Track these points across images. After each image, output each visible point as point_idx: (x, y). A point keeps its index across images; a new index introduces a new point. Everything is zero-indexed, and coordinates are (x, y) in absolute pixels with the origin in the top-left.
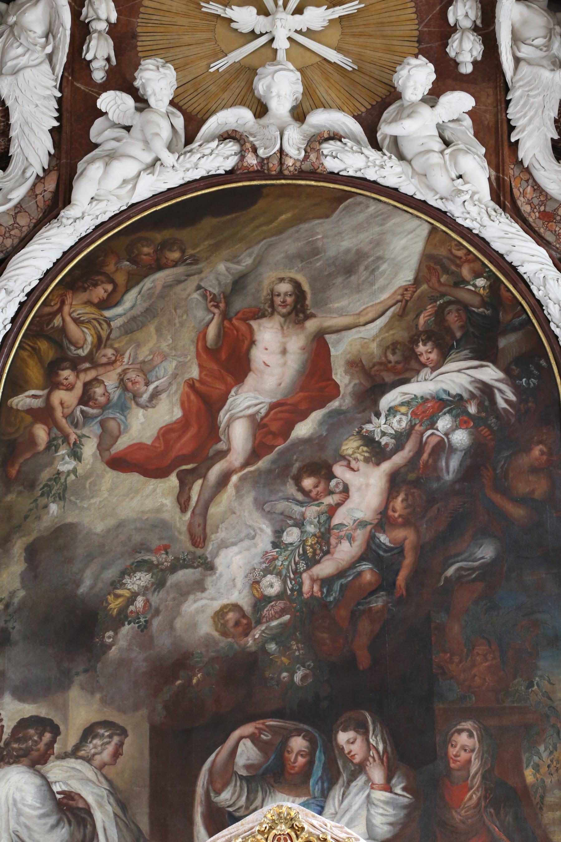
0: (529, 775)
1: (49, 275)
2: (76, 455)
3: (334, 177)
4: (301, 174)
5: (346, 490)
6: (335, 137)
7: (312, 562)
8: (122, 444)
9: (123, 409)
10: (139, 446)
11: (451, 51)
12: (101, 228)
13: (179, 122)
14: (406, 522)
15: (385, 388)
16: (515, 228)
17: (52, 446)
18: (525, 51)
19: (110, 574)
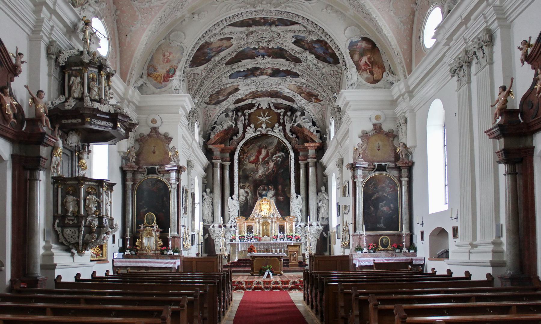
0: (285, 190)
1: (243, 145)
2: (246, 162)
3: (269, 134)
4: (266, 134)
6: (269, 131)
7: (267, 171)
8: (250, 161)
10: (251, 161)
11: (280, 121)
12: (248, 140)
13: (255, 129)
14: (275, 168)
15: (274, 155)
17: (244, 161)
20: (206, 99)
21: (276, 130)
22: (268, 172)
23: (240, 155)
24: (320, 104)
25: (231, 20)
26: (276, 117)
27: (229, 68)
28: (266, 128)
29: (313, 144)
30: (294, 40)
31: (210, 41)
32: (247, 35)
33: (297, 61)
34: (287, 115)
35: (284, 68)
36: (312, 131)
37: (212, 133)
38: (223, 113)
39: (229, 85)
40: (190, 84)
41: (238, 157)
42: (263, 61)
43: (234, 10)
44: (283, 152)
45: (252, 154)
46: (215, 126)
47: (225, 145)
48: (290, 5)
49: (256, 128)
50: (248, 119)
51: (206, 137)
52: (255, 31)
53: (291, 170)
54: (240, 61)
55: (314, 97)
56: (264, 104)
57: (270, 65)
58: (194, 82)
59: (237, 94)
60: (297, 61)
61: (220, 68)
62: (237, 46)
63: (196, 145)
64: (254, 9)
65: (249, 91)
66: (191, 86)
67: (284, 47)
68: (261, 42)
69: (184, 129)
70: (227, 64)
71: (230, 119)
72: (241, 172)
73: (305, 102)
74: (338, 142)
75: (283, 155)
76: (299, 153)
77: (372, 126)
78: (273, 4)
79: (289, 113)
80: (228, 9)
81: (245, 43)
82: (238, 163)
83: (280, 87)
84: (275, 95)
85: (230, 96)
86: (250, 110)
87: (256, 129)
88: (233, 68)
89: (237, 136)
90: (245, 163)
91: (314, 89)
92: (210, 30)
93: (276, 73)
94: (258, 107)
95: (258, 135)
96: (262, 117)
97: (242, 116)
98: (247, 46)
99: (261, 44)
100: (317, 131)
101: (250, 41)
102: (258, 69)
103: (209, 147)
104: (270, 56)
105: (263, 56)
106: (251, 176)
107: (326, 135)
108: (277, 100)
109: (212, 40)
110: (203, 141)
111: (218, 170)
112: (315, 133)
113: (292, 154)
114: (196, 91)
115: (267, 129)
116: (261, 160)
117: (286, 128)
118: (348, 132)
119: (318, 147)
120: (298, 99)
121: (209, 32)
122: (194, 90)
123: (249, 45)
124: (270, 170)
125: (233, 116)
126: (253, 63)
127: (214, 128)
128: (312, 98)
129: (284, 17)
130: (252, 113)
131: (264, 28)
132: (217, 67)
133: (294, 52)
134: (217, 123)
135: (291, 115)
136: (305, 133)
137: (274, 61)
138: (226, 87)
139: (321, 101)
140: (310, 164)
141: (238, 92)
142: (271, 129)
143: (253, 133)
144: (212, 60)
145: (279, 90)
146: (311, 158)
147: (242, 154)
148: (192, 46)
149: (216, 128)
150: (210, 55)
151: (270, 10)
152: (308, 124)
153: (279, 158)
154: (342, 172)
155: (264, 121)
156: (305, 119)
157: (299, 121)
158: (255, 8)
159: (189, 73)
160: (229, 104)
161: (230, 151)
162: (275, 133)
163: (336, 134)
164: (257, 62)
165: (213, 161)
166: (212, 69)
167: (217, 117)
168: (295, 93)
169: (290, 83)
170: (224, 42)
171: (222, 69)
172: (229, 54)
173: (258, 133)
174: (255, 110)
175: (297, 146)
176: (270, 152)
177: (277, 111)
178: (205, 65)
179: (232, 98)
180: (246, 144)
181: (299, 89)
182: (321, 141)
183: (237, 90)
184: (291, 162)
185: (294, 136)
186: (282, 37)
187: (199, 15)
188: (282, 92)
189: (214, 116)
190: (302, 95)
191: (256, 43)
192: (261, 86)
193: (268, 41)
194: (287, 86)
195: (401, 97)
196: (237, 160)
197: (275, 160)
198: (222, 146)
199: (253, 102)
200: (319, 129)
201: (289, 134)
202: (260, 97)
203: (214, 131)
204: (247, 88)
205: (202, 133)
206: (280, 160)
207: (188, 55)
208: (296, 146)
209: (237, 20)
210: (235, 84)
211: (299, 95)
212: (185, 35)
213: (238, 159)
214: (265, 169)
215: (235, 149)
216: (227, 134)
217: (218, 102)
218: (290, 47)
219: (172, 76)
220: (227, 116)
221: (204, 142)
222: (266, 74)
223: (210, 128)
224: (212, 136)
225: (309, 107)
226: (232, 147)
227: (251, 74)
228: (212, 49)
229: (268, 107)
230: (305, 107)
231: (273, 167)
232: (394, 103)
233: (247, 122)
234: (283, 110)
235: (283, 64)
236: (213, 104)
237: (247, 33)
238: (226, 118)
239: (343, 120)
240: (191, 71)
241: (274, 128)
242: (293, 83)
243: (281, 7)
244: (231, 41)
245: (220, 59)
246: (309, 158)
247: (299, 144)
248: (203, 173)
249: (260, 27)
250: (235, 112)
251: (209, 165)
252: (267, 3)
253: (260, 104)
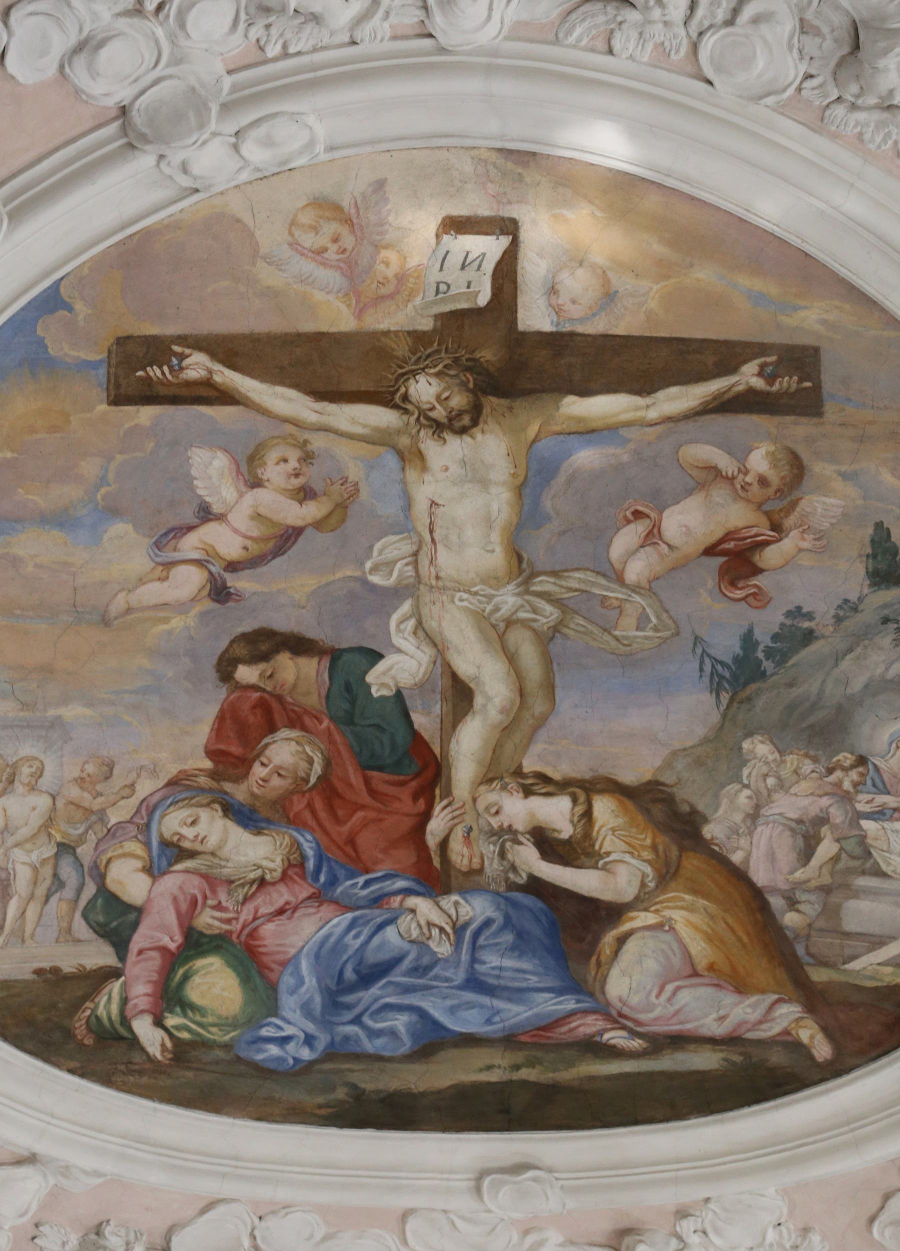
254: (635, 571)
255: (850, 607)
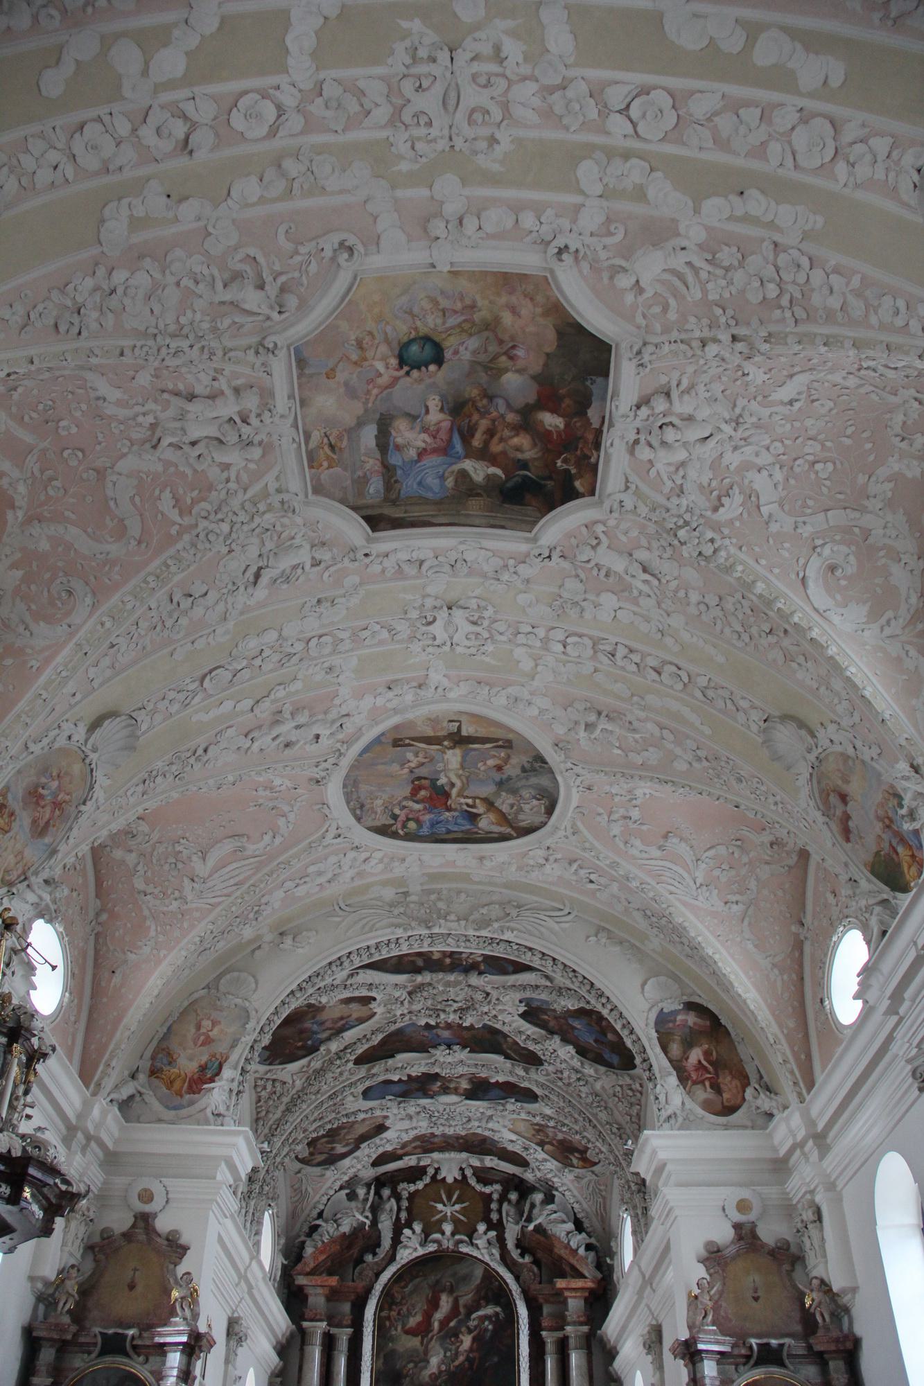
1: (390, 1279)
2: (396, 1330)
3: (461, 1253)
4: (453, 1251)
5: (462, 1342)
6: (462, 1241)
7: (453, 1361)
9: (408, 1317)
12: (403, 1266)
16: (505, 1269)
18: (510, 1219)
19: (404, 1363)
20: (299, 1148)
21: (481, 1242)
22: (457, 1363)
23: (380, 1308)
24: (593, 1172)
25: (371, 954)
26: (481, 1205)
27: (363, 1071)
28: (453, 1234)
29: (579, 1283)
30: (522, 1009)
31: (320, 1002)
32: (410, 993)
33: (532, 1060)
34: (509, 1202)
35: (501, 1079)
36: (573, 1244)
37: (308, 1243)
38: (341, 1188)
39: (361, 1116)
40: (261, 1107)
41: (375, 1314)
42: (449, 1059)
43: (379, 933)
44: (497, 1303)
45: (413, 1306)
46: (317, 1222)
47: (342, 1279)
48: (512, 924)
49: (426, 1233)
50: (407, 1209)
51: (292, 1253)
52: (430, 984)
53: (521, 1359)
54: (392, 1056)
55: (576, 1154)
56: (450, 1171)
57: (466, 1069)
58: (271, 1102)
59: (381, 1139)
60: (532, 1060)
61: (339, 1070)
62: (386, 1018)
63: (259, 1275)
64: (428, 932)
65: (412, 1134)
66: (263, 1113)
67: (498, 1026)
68: (444, 1011)
69: (229, 1223)
70: (359, 1061)
71: (360, 1205)
72: (381, 1361)
73: (553, 1167)
74: (644, 1276)
75: (497, 1314)
76: (540, 1308)
77: (732, 1231)
78: (473, 922)
79: (513, 1196)
80: (367, 928)
81: (406, 1011)
82: (374, 1332)
83: (490, 1125)
84: (478, 1145)
85: (362, 1146)
86: (414, 1183)
87: (427, 1236)
88: (373, 1071)
89: (375, 1254)
90: (394, 1333)
91: (577, 1132)
92: (319, 974)
93: (479, 1089)
94: (434, 1178)
95: (431, 1253)
96: (445, 1205)
97: (393, 1200)
98: (410, 1019)
99: (442, 1016)
100: (589, 1247)
101: (416, 1007)
102: (436, 1076)
103: (296, 1283)
104: (464, 1047)
105: (449, 1047)
106: (407, 1376)
107: (612, 1259)
108: (482, 1161)
109: (324, 1000)
110: (283, 1264)
111: (314, 1351)
112: (582, 1251)
113: (522, 1311)
114: (274, 1127)
115: (457, 1237)
116: (436, 1325)
117: (507, 1235)
118: (667, 1249)
119: (591, 1291)
120: (537, 1160)
121: (315, 980)
122: (270, 1123)
123: (414, 1018)
124: (461, 1358)
125: (367, 1199)
126: (423, 1062)
127: (314, 1228)
128: (571, 1157)
129: (498, 952)
130: (417, 1191)
131: (452, 977)
132: (333, 1068)
133: (524, 1037)
134: (325, 1215)
135: (518, 1202)
136: (556, 1250)
137: (475, 1059)
138: (352, 1119)
139: (595, 1164)
140: (572, 1342)
141: (387, 1135)
142: (466, 1238)
143: (418, 1246)
144: (322, 1049)
145: (487, 1133)
146: (574, 1323)
147: (386, 1306)
148: (272, 1010)
149: (320, 1230)
150: (319, 1036)
151: (466, 936)
152: (564, 1226)
153: (486, 1323)
154: (659, 1366)
155: (449, 1214)
156: (555, 1212)
157: (541, 1218)
158: (429, 928)
159: (262, 1079)
160: (359, 1166)
161: (353, 1297)
162: (478, 1248)
163: (639, 1252)
164: (433, 1060)
165: (305, 1324)
166: (319, 1073)
167: (326, 1198)
168: (528, 1143)
169: (515, 1116)
170: (354, 1006)
171: (346, 1074)
172: (365, 1036)
173: (432, 1248)
174: (426, 1185)
175: (535, 1287)
176: (462, 1302)
177: (483, 1190)
178: (304, 1062)
179: (367, 1151)
180: (398, 1278)
181: (538, 1131)
182: (599, 1276)
183: (381, 1128)
184: (518, 1334)
185: (527, 1259)
186: (494, 1001)
187: (296, 939)
188: (496, 1138)
189: (318, 1196)
190: (547, 1147)
191: (431, 1013)
192: (442, 1121)
193: (461, 1009)
194: (507, 1123)
195: (798, 1152)
196: (371, 1324)
197: (476, 1327)
198: (333, 1281)
199: (422, 1164)
200: (593, 1241)
201: (515, 1254)
202: (441, 1149)
203: (315, 1236)
204: (406, 1124)
205: (283, 1241)
206: (490, 1327)
207: (258, 1030)
208: (533, 1287)
209: (385, 954)
210: (378, 1113)
211: (539, 1149)
212: (257, 982)
213: (374, 1321)
214: (448, 1354)
215: (369, 1291)
216: (349, 1247)
217: (332, 1160)
218: (514, 1025)
219: (212, 1080)
220: (352, 1196)
221: (284, 1267)
222: (456, 1091)
223: (306, 1229)
224: (309, 1250)
225: (565, 1181)
226: (360, 1285)
227: (418, 1090)
228: (323, 1023)
229: (459, 1178)
230: (555, 1180)
231: (471, 1350)
232: (780, 1167)
233: (403, 1215)
234: (498, 1187)
235: (498, 1068)
236: (319, 1164)
237: (410, 989)
238: (347, 1204)
239: (653, 1212)
240: (266, 1073)
241: (475, 1235)
242: (523, 1116)
243: (490, 928)
244: (371, 1006)
245: (342, 1048)
246: (568, 1325)
247: (540, 1283)
248: (274, 1359)
249: (441, 975)
250: (373, 1187)
251: (292, 1335)
252: (459, 920)
253: (439, 1168)
254: (482, 768)
255: (517, 776)
